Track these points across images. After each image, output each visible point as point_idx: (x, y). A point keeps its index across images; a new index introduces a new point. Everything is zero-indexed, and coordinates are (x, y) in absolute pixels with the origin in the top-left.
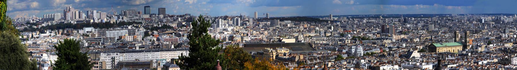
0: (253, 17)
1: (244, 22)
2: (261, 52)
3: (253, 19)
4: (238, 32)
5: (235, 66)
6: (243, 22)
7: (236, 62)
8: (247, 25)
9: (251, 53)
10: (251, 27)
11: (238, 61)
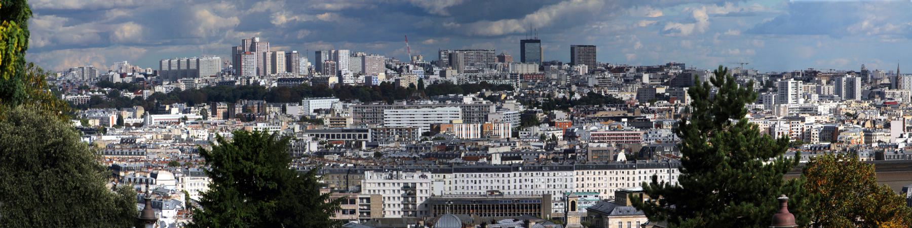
1: (876, 88)
4: (855, 116)
6: (872, 88)
7: (849, 222)
8: (887, 96)
10: (907, 105)
11: (854, 221)
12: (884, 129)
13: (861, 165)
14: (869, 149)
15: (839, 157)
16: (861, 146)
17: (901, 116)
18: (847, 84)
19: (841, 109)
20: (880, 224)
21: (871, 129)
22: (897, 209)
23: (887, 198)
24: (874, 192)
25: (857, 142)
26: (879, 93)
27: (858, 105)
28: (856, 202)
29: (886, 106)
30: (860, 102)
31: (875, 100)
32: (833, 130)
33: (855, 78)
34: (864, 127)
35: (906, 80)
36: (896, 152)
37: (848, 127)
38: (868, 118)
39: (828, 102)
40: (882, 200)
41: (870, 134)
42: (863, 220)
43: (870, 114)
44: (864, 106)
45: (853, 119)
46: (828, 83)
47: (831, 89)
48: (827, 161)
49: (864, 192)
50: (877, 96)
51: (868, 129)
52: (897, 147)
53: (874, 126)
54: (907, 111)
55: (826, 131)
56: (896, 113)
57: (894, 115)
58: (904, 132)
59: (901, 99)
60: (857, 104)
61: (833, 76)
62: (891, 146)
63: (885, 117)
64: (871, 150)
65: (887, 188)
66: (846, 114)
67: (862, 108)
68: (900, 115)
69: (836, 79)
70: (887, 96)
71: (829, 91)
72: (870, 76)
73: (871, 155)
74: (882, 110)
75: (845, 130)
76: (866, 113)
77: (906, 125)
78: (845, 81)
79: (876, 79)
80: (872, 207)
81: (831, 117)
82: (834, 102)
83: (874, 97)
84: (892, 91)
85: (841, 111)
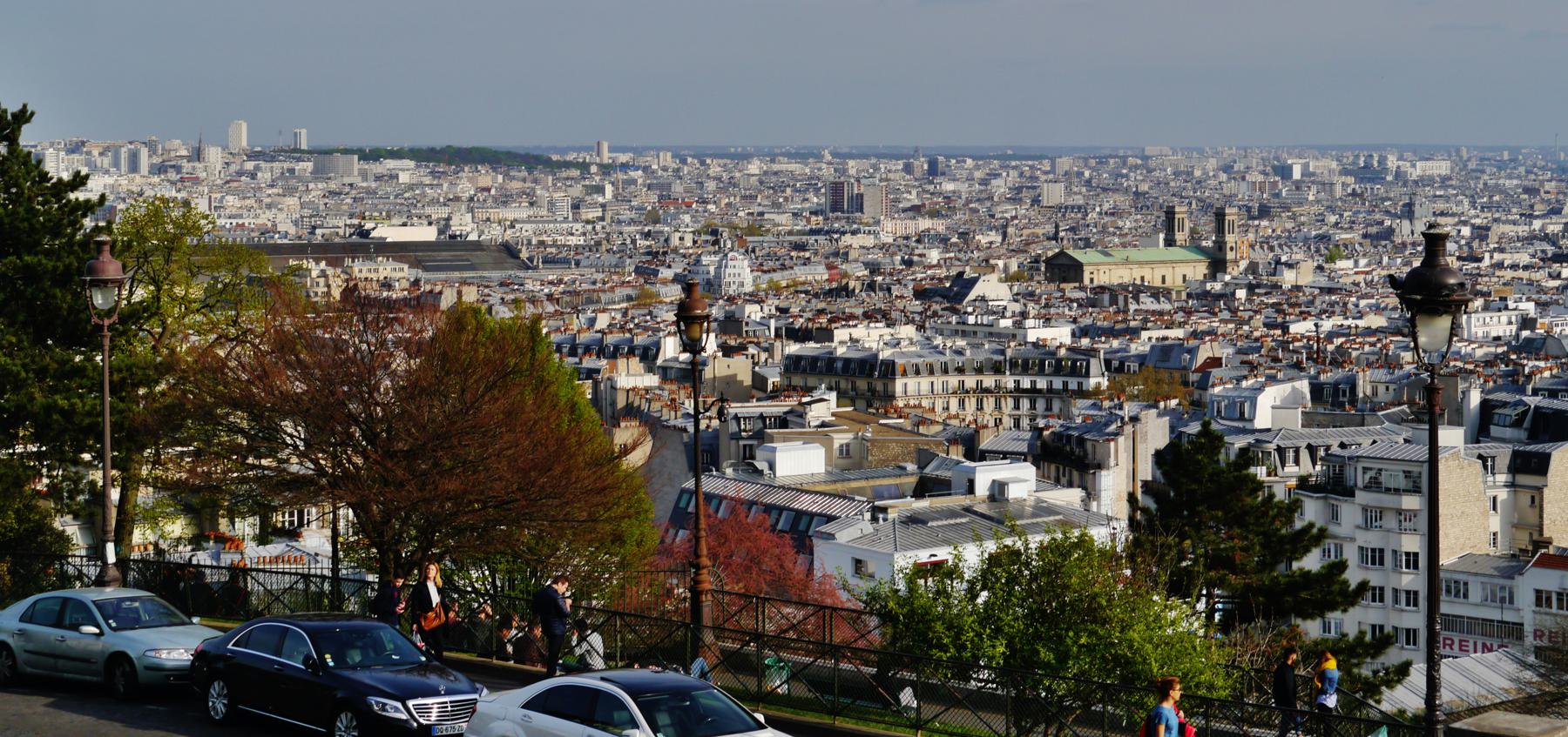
6: (164, 161)
50: (170, 170)
59: (205, 174)
77: (213, 205)
79: (170, 150)
83: (166, 172)
84: (191, 164)
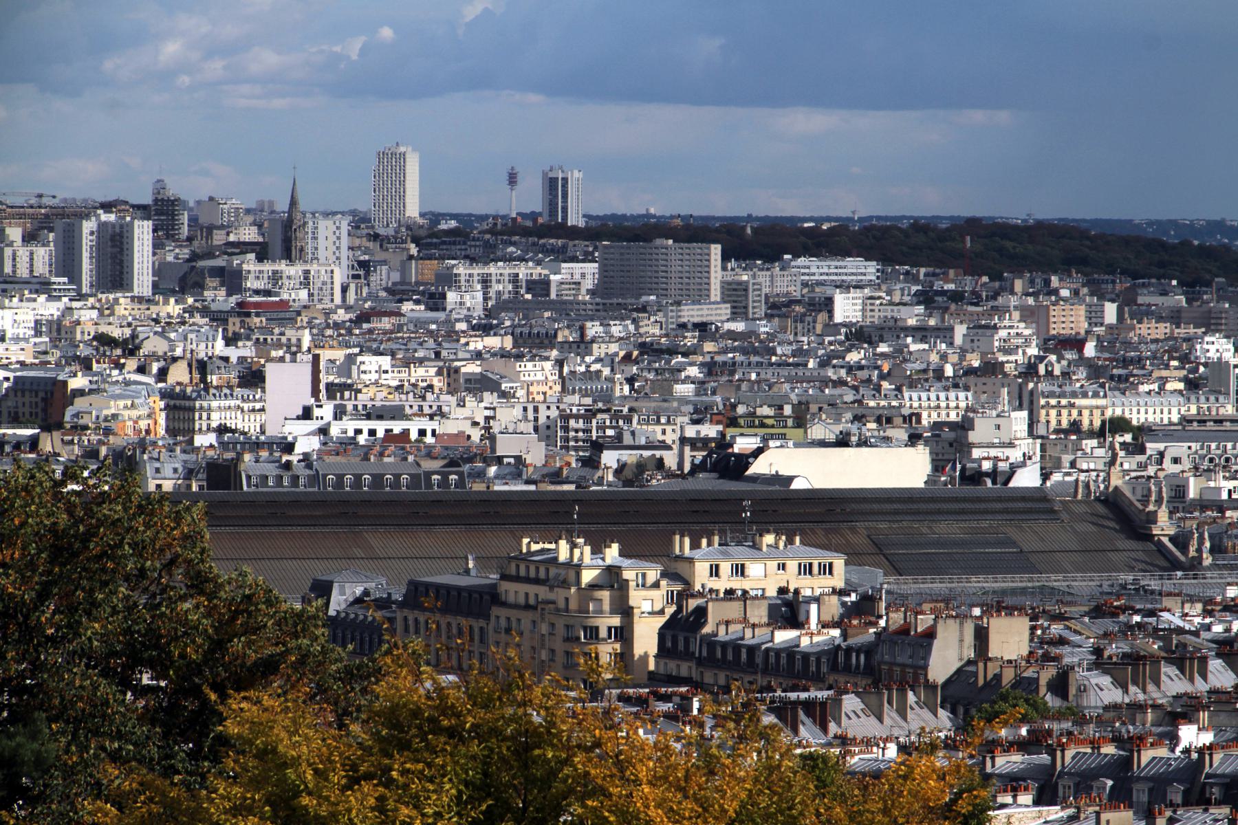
0: (364, 204)
1: (210, 255)
2: (463, 581)
3: (359, 222)
4: (130, 347)
5: (96, 733)
7: (105, 688)
8: (251, 283)
9: (323, 589)
10: (327, 314)
11: (125, 683)
12: (238, 391)
13: (151, 505)
14: (184, 451)
15: (70, 474)
16: (154, 443)
17: (305, 348)
18: (98, 243)
19: (78, 323)
20: (223, 697)
21: (189, 389)
22: (288, 652)
23: (250, 614)
24: (202, 592)
25: (137, 431)
26: (219, 272)
27: (139, 311)
28: (135, 622)
29: (248, 315)
30: (149, 301)
31: (206, 293)
32: (49, 388)
33: (131, 224)
34: (165, 381)
35: (321, 234)
36: (288, 466)
37: (104, 381)
38: (179, 352)
39: (29, 300)
40: (233, 618)
41: (187, 403)
42: (163, 684)
43: (186, 339)
44: (162, 314)
45: (124, 356)
46: (30, 238)
47: (44, 256)
48: (26, 488)
49: (163, 591)
51: (178, 389)
52: (289, 448)
53: (203, 379)
54: (329, 332)
55: (23, 392)
56: (284, 339)
57: (279, 345)
58: (318, 400)
60: (137, 306)
61: (47, 216)
62: (269, 445)
63: (245, 350)
64: (192, 457)
65: (250, 579)
66: (95, 338)
67: (157, 321)
68: (299, 346)
69: (59, 224)
70: (251, 283)
71: (32, 265)
72: (185, 218)
73: (189, 474)
74: (231, 328)
75: (91, 391)
76: (173, 335)
78: (92, 233)
80: (194, 642)
81: (42, 348)
82: (51, 298)
85: (79, 329)
